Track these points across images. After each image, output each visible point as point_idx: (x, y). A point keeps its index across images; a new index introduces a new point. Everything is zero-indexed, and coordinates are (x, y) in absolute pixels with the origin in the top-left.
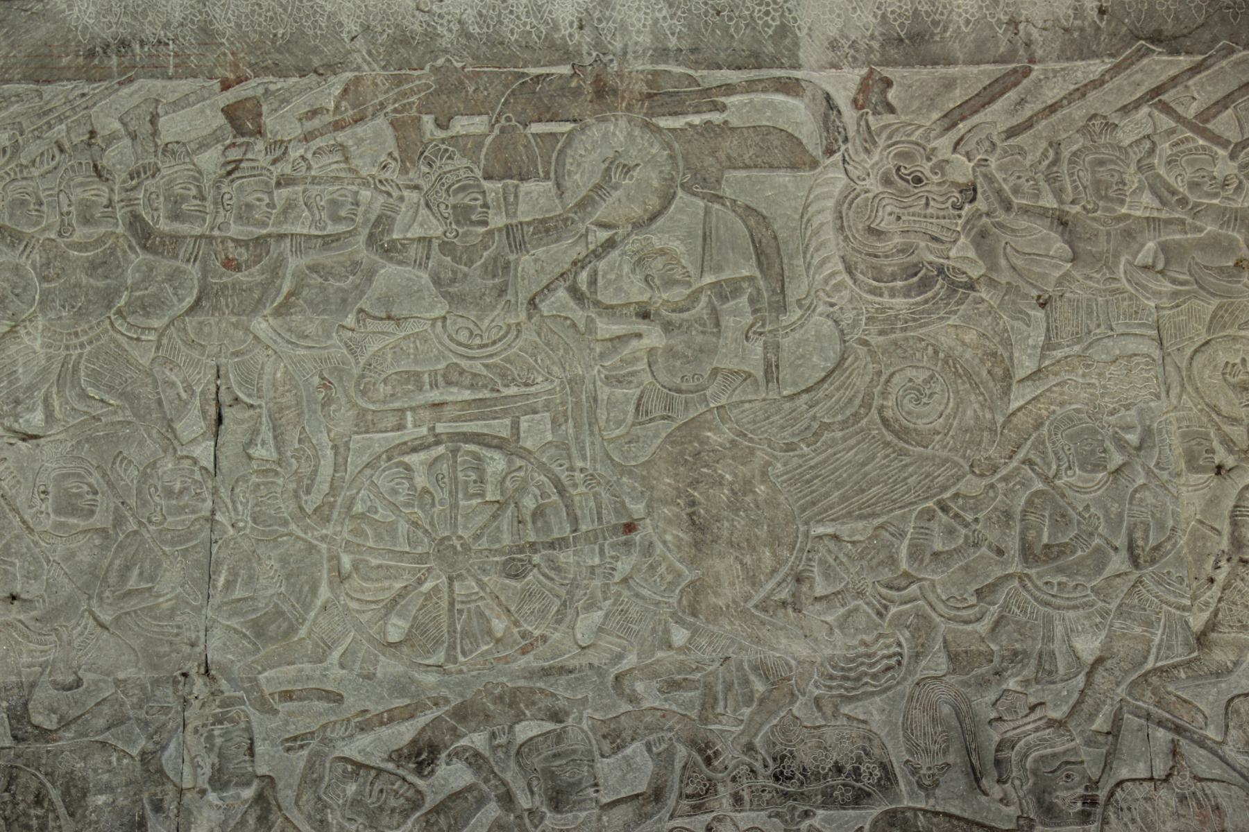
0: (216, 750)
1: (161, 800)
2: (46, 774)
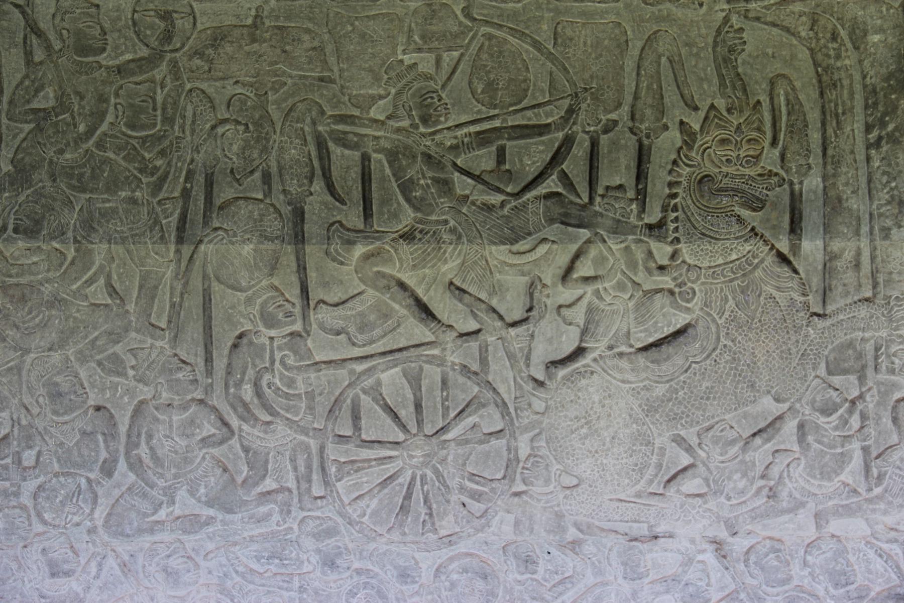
2: (838, 19)
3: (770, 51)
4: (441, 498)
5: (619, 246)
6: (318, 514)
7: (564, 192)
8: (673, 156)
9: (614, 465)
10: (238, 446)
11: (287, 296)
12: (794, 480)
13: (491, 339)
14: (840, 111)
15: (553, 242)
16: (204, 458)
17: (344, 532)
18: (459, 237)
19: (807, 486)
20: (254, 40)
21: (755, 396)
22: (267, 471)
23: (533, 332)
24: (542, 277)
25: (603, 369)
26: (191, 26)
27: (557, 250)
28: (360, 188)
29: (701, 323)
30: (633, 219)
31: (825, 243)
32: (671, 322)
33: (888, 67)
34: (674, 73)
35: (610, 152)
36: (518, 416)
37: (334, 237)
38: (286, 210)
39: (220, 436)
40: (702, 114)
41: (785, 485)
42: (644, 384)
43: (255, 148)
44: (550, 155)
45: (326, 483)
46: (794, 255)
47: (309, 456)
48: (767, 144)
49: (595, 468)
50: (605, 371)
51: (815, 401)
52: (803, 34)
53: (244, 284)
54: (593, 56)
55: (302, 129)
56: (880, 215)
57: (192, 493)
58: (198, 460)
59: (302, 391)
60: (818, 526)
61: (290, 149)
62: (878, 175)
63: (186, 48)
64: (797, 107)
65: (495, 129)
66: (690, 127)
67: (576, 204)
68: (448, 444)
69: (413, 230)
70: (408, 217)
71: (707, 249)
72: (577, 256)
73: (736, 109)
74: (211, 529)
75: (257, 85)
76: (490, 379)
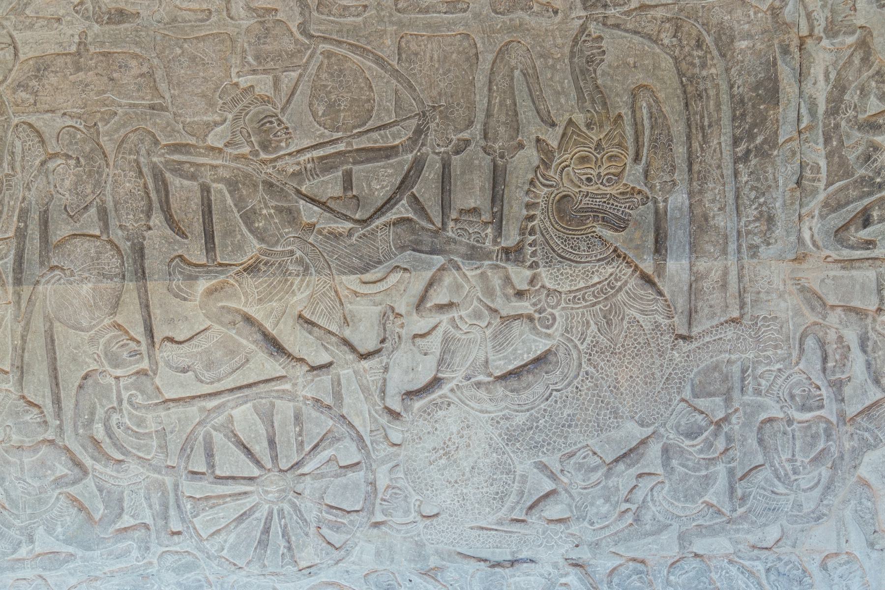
0: (829, 6)
1: (788, 45)
3: (631, 60)
4: (299, 531)
5: (474, 273)
6: (178, 549)
7: (415, 218)
8: (530, 176)
9: (474, 494)
10: (93, 484)
11: (132, 334)
12: (657, 504)
13: (345, 373)
14: (706, 123)
15: (405, 269)
16: (57, 498)
17: (204, 565)
18: (307, 269)
19: (671, 509)
20: (78, 69)
21: (617, 422)
22: (123, 510)
23: (387, 364)
24: (396, 306)
25: (460, 400)
26: (12, 57)
27: (410, 277)
28: (201, 220)
29: (562, 350)
30: (488, 244)
31: (690, 262)
32: (531, 349)
33: (756, 75)
34: (528, 87)
35: (463, 173)
36: (373, 448)
37: (174, 273)
38: (125, 246)
39: (72, 477)
40: (559, 130)
41: (648, 508)
42: (503, 413)
43: (88, 183)
44: (399, 179)
45: (183, 520)
46: (659, 277)
47: (163, 494)
48: (629, 160)
49: (455, 497)
50: (463, 402)
51: (680, 425)
52: (666, 41)
53: (85, 324)
54: (441, 71)
55: (137, 162)
56: (748, 233)
57: (50, 531)
58: (53, 500)
59: (153, 430)
60: (682, 547)
61: (122, 184)
62: (746, 191)
63: (9, 81)
64: (660, 121)
65: (340, 153)
66: (547, 144)
67: (428, 230)
68: (303, 478)
69: (258, 261)
70: (254, 247)
71: (568, 273)
72: (430, 284)
73: (595, 124)
74: (71, 565)
75: (85, 116)
76: (344, 412)
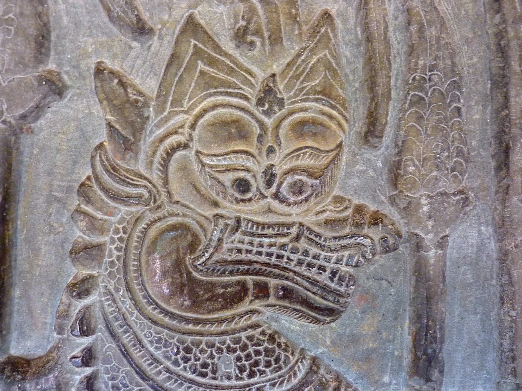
40: (161, 48)
48: (348, 134)
64: (431, 32)
73: (258, 33)
